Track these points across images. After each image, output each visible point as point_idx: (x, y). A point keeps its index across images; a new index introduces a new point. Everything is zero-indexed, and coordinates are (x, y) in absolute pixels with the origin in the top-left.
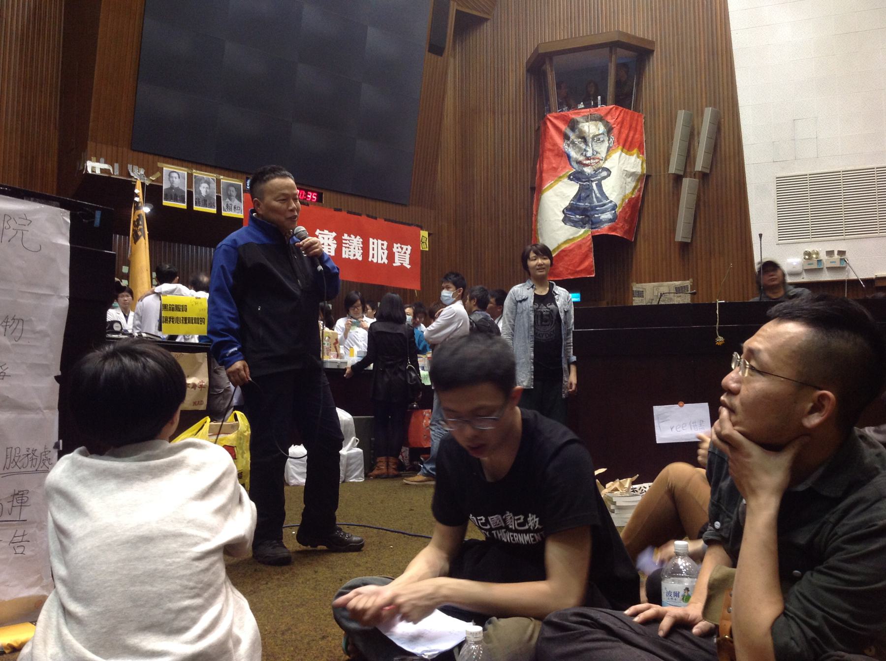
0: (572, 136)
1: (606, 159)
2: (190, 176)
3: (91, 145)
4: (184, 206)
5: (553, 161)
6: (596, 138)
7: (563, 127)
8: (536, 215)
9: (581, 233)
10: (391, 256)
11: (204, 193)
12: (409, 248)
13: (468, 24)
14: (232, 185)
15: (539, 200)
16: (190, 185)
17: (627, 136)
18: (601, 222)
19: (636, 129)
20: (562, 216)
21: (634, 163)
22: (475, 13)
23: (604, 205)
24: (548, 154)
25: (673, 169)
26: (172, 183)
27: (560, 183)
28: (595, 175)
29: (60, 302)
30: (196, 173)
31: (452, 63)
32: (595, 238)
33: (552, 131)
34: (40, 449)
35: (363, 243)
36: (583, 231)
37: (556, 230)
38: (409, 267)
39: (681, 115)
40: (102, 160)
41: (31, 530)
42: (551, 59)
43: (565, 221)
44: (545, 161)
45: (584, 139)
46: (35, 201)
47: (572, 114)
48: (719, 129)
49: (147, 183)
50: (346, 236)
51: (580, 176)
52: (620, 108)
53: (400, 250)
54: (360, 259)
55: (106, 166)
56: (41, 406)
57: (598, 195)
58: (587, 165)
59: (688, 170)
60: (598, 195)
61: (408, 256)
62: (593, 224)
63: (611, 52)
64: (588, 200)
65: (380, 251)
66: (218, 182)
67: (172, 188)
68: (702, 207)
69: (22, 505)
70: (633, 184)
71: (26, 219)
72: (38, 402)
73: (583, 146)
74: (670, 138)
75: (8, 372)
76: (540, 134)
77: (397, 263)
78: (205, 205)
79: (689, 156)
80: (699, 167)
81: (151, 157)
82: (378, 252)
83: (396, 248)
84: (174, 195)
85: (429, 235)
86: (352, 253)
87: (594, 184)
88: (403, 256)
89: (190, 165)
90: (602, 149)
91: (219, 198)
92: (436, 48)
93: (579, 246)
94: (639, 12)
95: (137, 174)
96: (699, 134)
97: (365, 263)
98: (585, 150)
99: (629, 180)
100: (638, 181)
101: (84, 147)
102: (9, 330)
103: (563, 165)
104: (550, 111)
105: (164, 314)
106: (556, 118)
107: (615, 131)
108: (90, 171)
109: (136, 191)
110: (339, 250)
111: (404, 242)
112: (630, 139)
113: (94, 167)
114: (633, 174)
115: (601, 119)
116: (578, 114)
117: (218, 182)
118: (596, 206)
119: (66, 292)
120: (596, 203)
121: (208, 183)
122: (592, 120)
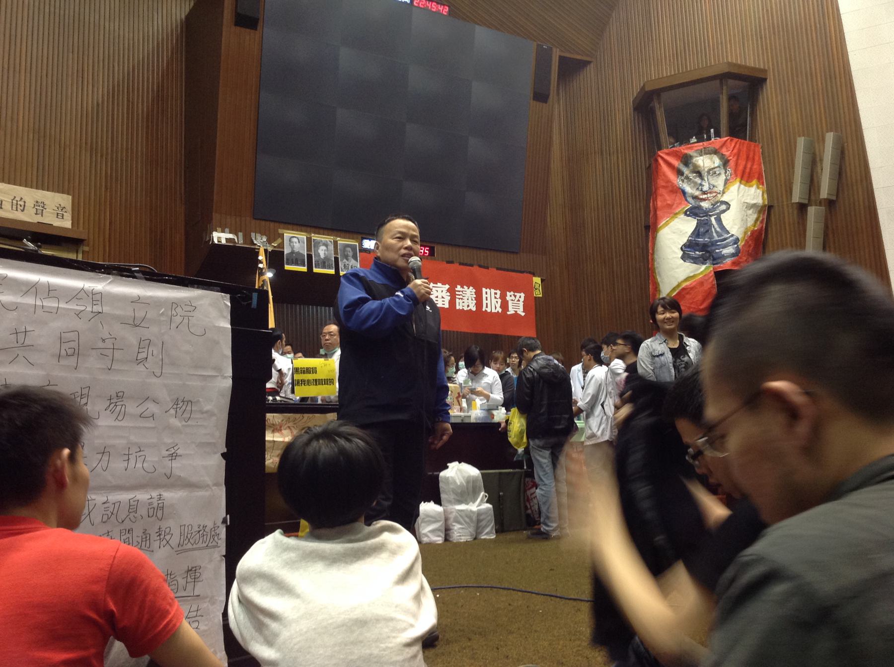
0: (686, 171)
1: (724, 193)
2: (309, 240)
3: (216, 217)
4: (304, 269)
5: (667, 197)
6: (712, 172)
7: (676, 163)
8: (653, 254)
9: (702, 269)
10: (505, 305)
11: (322, 256)
12: (523, 295)
13: (571, 68)
14: (348, 246)
15: (654, 238)
16: (309, 248)
17: (745, 168)
18: (724, 257)
19: (754, 159)
20: (680, 253)
21: (754, 194)
22: (579, 57)
23: (725, 239)
24: (662, 191)
25: (796, 198)
26: (293, 247)
27: (676, 220)
28: (714, 209)
29: (224, 382)
30: (315, 237)
31: (557, 107)
32: (720, 275)
33: (664, 168)
34: (210, 525)
35: (476, 293)
36: (704, 267)
37: (675, 268)
38: (523, 314)
39: (801, 142)
40: (227, 230)
41: (204, 605)
42: (659, 95)
43: (685, 257)
44: (659, 199)
45: (699, 174)
46: (198, 288)
47: (684, 149)
48: (842, 153)
49: (270, 249)
50: (459, 288)
51: (697, 211)
52: (735, 140)
53: (513, 298)
54: (474, 309)
55: (231, 236)
56: (210, 483)
57: (718, 229)
58: (704, 200)
59: (813, 198)
60: (718, 229)
61: (521, 304)
62: (714, 259)
63: (721, 83)
64: (707, 235)
65: (494, 301)
66: (335, 243)
67: (293, 252)
68: (831, 236)
69: (195, 580)
70: (755, 216)
71: (189, 304)
72: (208, 480)
73: (698, 180)
74: (791, 165)
75: (179, 452)
76: (652, 171)
77: (511, 311)
78: (324, 267)
79: (812, 183)
80: (824, 193)
81: (272, 224)
82: (492, 301)
83: (509, 296)
84: (296, 259)
85: (542, 281)
86: (466, 304)
87: (713, 219)
88: (517, 304)
89: (309, 229)
90: (719, 182)
91: (336, 259)
92: (541, 96)
93: (701, 283)
94: (748, 41)
95: (260, 242)
96: (821, 160)
97: (479, 313)
98: (701, 185)
99: (750, 212)
100: (759, 212)
101: (210, 220)
102: (180, 412)
103: (678, 201)
104: (660, 149)
105: (296, 377)
106: (668, 154)
107: (732, 163)
108: (216, 241)
109: (260, 258)
110: (452, 302)
111: (516, 290)
112: (748, 170)
113: (220, 237)
114: (754, 206)
115: (715, 152)
116: (691, 148)
117: (335, 243)
118: (717, 241)
119: (229, 372)
120: (716, 238)
121: (326, 245)
122: (706, 154)
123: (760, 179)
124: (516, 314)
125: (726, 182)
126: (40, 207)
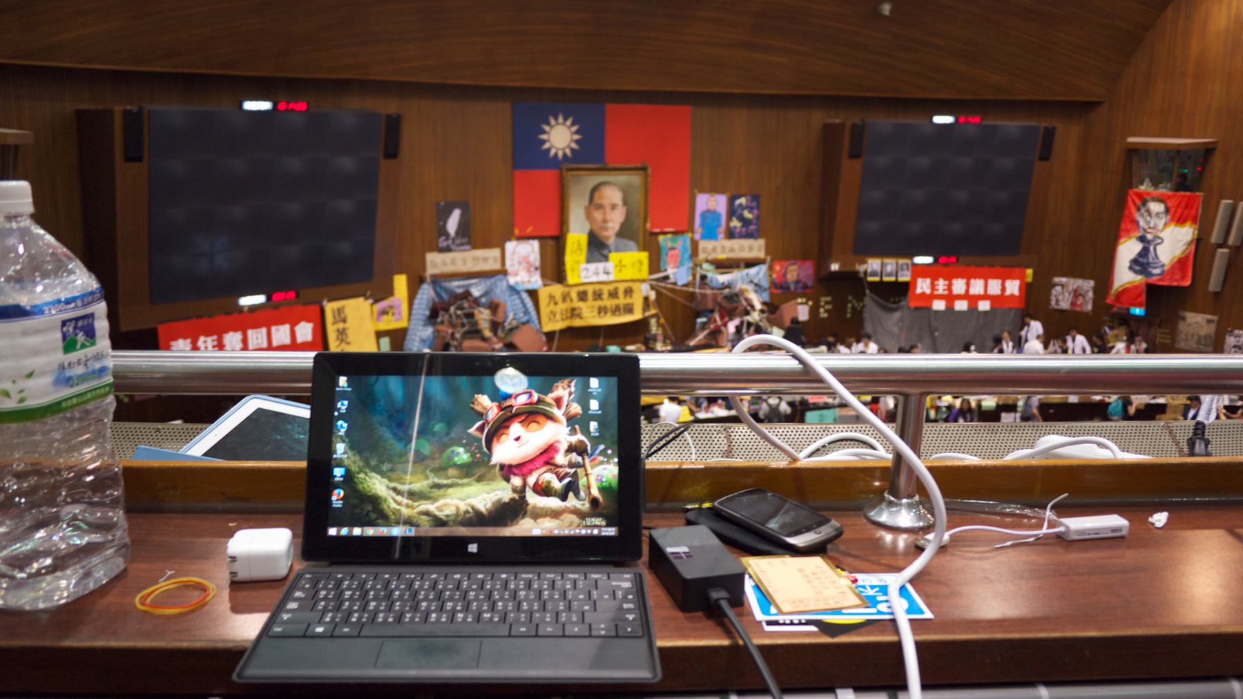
0: (1143, 210)
6: (1157, 214)
10: (1003, 289)
30: (886, 261)
43: (1131, 268)
45: (1150, 215)
77: (1008, 292)
82: (994, 287)
84: (874, 274)
87: (1152, 248)
88: (1013, 287)
90: (1161, 223)
93: (1136, 287)
107: (1173, 210)
110: (967, 290)
111: (1013, 278)
113: (835, 267)
123: (1194, 221)
124: (1012, 296)
125: (1166, 225)
126: (751, 249)
